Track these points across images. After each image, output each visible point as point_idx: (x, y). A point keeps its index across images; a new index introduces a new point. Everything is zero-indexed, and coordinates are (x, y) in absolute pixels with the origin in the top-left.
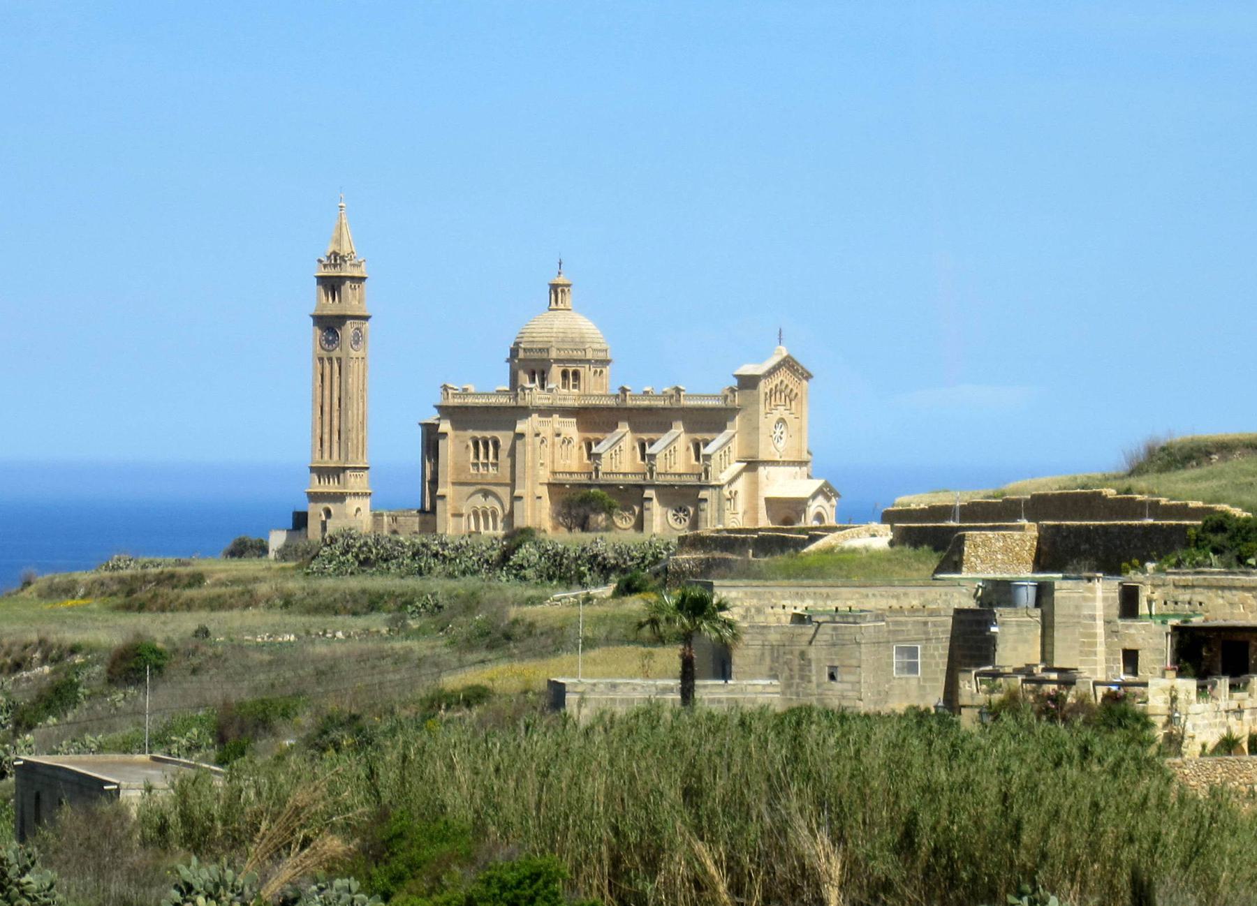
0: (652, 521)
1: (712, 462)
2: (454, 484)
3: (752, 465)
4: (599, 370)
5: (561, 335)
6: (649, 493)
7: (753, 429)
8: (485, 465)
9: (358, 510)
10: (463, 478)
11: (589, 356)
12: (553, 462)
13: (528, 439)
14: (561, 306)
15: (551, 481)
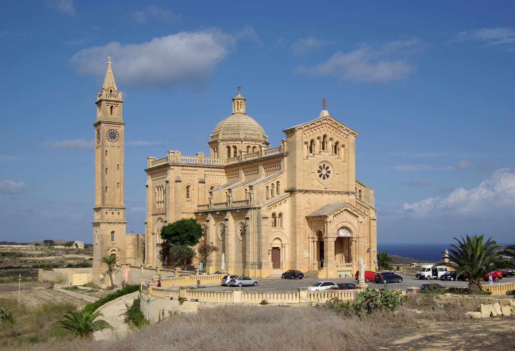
0: (228, 235)
1: (255, 191)
2: (152, 215)
3: (291, 192)
4: (252, 146)
5: (227, 126)
6: (229, 216)
7: (293, 168)
8: (160, 202)
9: (113, 232)
10: (156, 212)
11: (242, 137)
12: (198, 200)
13: (172, 184)
14: (237, 111)
15: (197, 211)
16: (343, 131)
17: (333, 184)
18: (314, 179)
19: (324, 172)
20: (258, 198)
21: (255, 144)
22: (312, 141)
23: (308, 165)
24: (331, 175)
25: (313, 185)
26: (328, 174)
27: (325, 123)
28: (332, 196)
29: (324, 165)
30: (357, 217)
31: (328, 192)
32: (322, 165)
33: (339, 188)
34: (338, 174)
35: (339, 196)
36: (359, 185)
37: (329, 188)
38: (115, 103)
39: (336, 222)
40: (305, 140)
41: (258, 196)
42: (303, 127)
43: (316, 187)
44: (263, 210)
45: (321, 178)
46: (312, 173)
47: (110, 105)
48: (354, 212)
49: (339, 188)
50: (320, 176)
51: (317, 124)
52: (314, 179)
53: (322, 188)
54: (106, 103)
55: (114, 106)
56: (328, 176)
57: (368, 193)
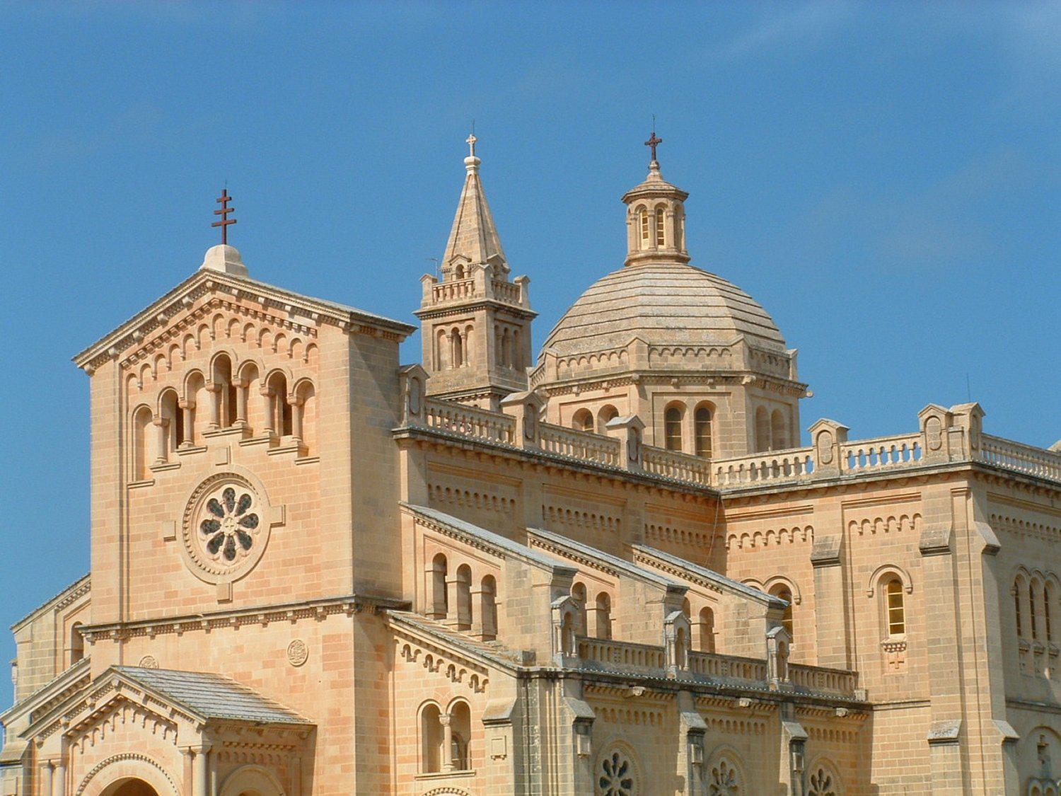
16: (286, 317)
17: (261, 575)
18: (177, 567)
19: (230, 525)
20: (32, 680)
21: (607, 394)
22: (170, 397)
23: (153, 509)
24: (258, 535)
25: (171, 595)
26: (248, 531)
27: (209, 303)
28: (250, 631)
29: (229, 494)
30: (172, 727)
31: (245, 617)
32: (218, 496)
33: (286, 590)
34: (281, 525)
35: (307, 624)
36: (478, 552)
37: (243, 595)
38: (464, 316)
39: (90, 760)
40: (136, 400)
41: (33, 673)
42: (108, 347)
43: (187, 602)
44: (12, 730)
45: (216, 556)
46: (167, 540)
47: (448, 329)
48: (150, 706)
49: (286, 590)
50: (213, 546)
51: (176, 319)
52: (177, 567)
53: (209, 599)
54: (435, 326)
55: (462, 328)
56: (247, 542)
57: (518, 584)
